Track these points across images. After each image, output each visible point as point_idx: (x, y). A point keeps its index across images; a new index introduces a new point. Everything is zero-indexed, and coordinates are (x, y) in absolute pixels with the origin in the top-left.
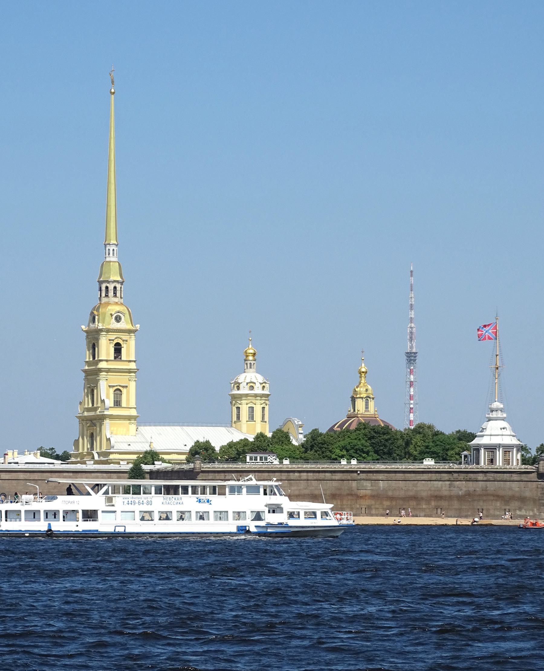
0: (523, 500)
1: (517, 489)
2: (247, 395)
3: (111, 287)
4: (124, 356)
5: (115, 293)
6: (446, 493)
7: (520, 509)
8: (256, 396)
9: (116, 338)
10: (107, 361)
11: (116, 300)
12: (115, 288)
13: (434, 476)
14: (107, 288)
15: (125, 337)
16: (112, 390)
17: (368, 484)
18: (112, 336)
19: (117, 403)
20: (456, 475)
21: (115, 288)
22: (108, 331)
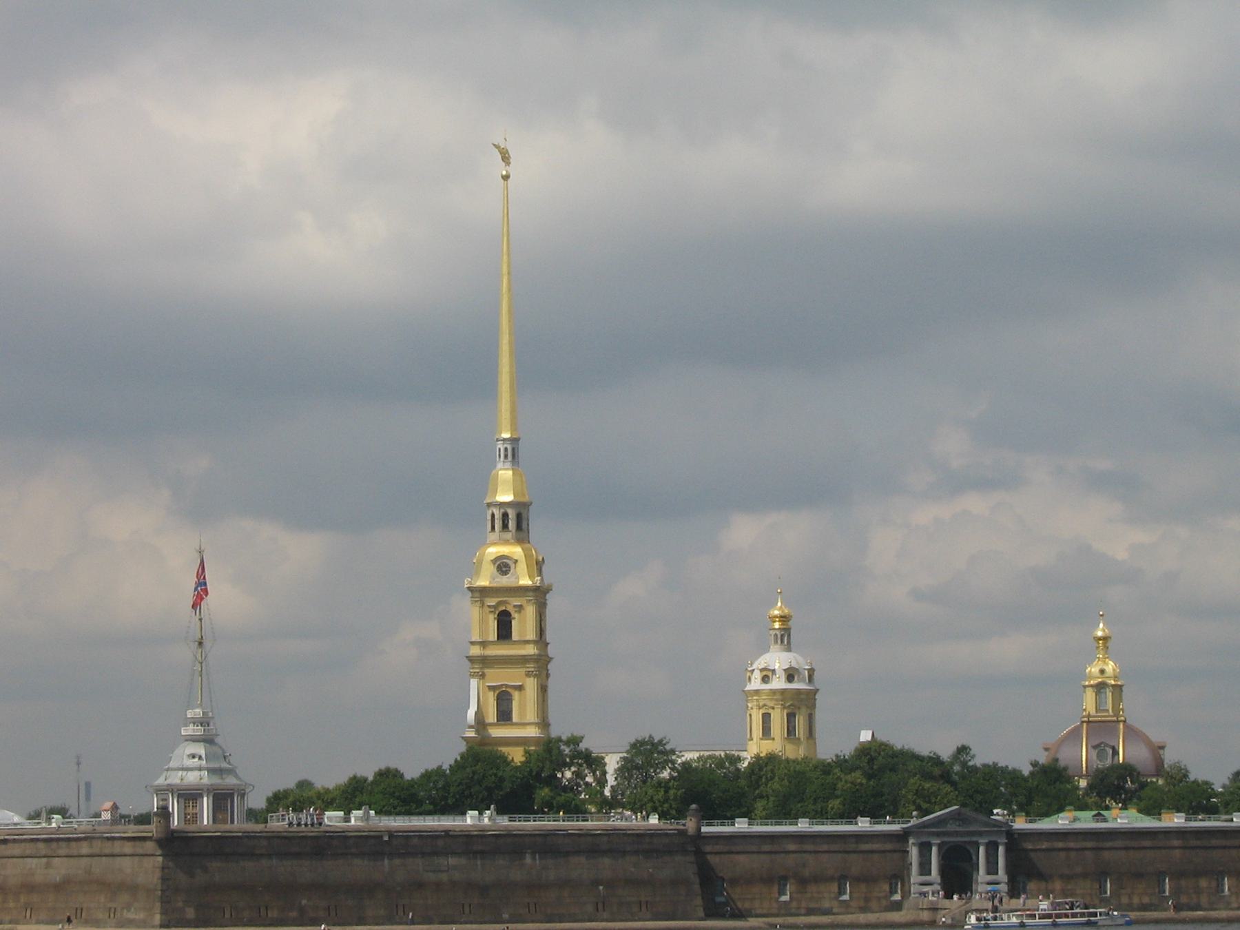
0: (132, 889)
2: (757, 692)
4: (515, 636)
5: (505, 526)
6: (39, 878)
7: (128, 907)
8: (773, 692)
9: (500, 603)
10: (484, 644)
11: (508, 535)
12: (505, 515)
13: (29, 849)
14: (493, 515)
18: (492, 602)
19: (504, 716)
20: (54, 845)
21: (505, 515)
22: (483, 592)
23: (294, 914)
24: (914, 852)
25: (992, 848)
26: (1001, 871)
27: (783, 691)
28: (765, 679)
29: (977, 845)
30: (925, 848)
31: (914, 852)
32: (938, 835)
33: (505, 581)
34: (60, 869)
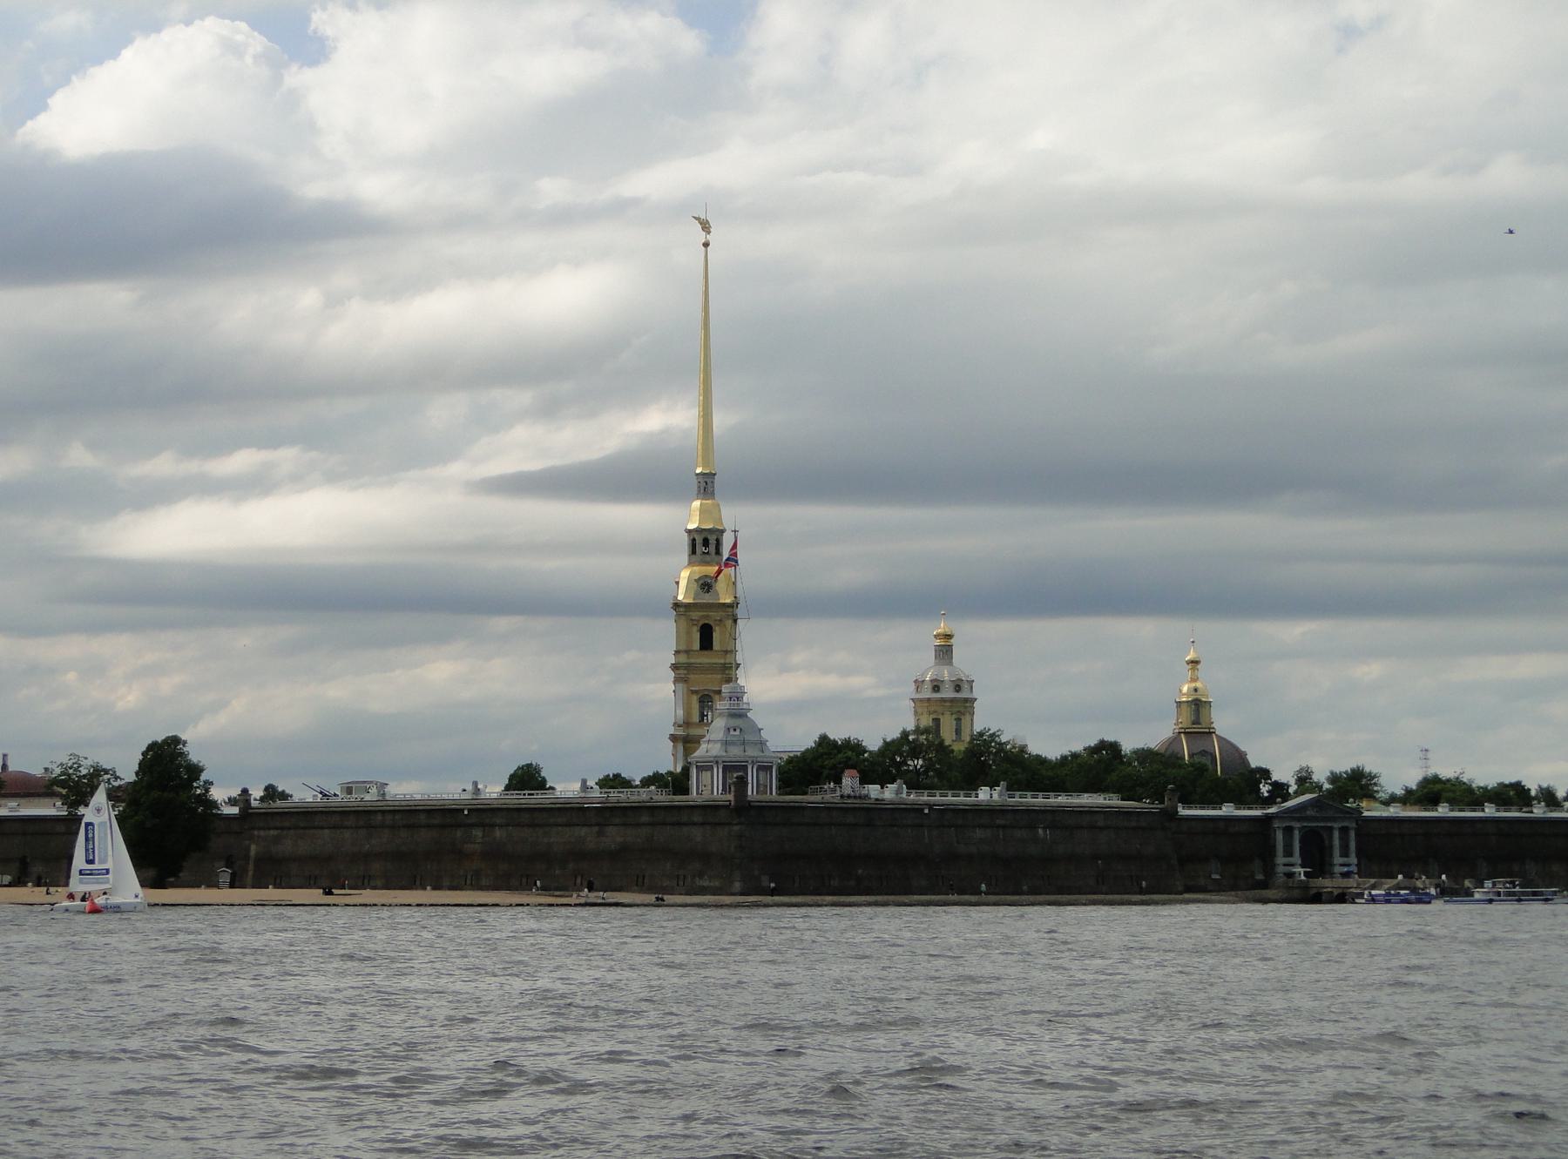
1: (699, 839)
3: (699, 541)
4: (716, 645)
8: (943, 700)
11: (708, 558)
15: (716, 615)
16: (695, 698)
17: (478, 833)
18: (695, 615)
23: (852, 883)
24: (1280, 836)
25: (1344, 831)
26: (1353, 855)
27: (952, 700)
28: (936, 688)
29: (1331, 829)
30: (1288, 831)
31: (1280, 836)
32: (1298, 819)
33: (707, 599)
34: (614, 836)
